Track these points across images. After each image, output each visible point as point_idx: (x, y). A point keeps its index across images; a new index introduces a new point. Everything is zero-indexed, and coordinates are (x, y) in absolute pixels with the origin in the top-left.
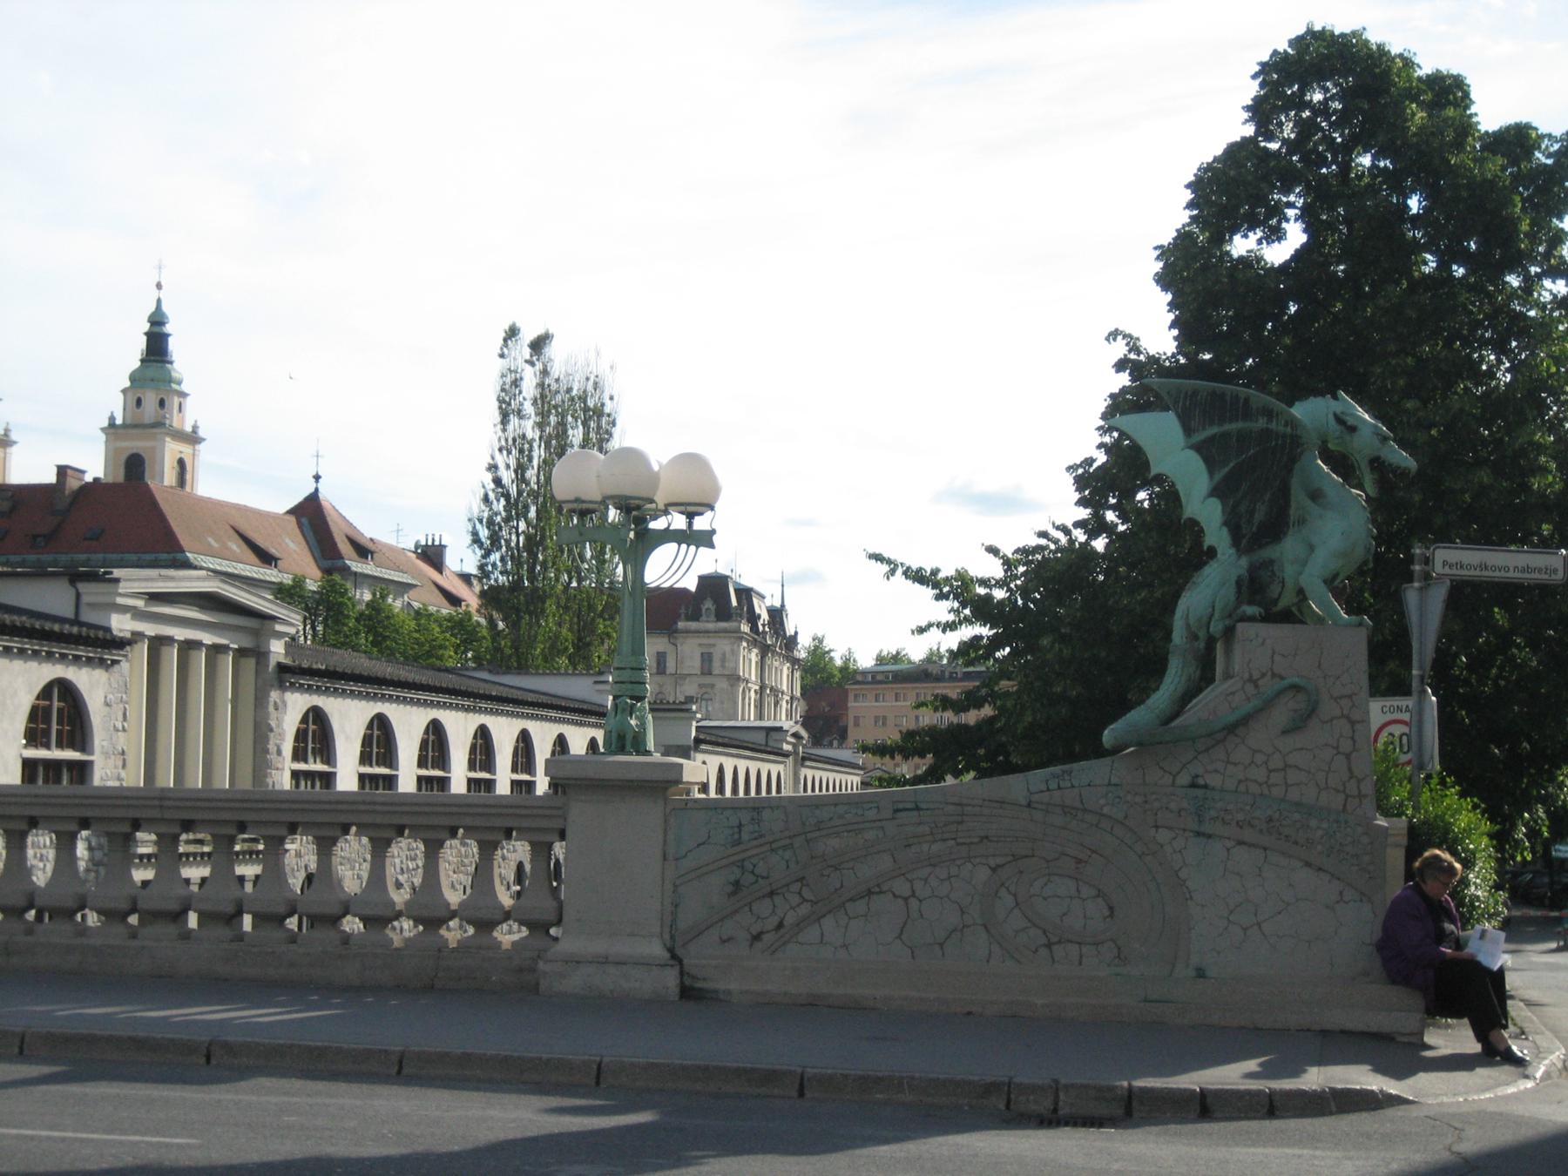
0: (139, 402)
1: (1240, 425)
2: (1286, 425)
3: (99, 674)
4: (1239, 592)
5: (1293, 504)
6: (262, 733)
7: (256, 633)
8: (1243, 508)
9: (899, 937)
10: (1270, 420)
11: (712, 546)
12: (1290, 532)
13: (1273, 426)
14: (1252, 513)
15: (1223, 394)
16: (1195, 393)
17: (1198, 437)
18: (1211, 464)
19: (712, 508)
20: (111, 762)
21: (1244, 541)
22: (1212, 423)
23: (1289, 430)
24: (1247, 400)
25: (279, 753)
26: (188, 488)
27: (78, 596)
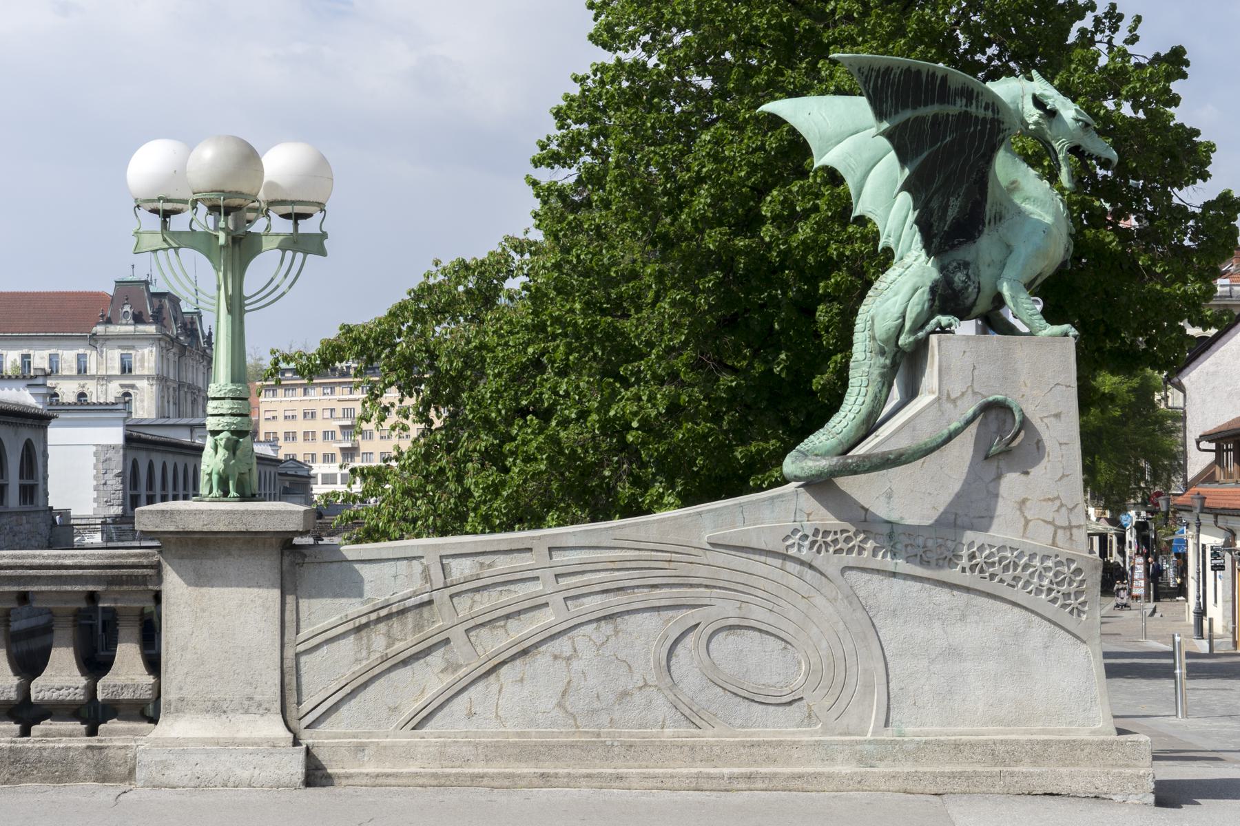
4: (932, 300)
5: (989, 201)
8: (935, 204)
9: (559, 705)
11: (322, 252)
12: (986, 230)
13: (972, 109)
14: (945, 209)
15: (919, 72)
16: (888, 70)
19: (321, 206)
21: (936, 241)
22: (905, 107)
23: (990, 114)
24: (944, 79)
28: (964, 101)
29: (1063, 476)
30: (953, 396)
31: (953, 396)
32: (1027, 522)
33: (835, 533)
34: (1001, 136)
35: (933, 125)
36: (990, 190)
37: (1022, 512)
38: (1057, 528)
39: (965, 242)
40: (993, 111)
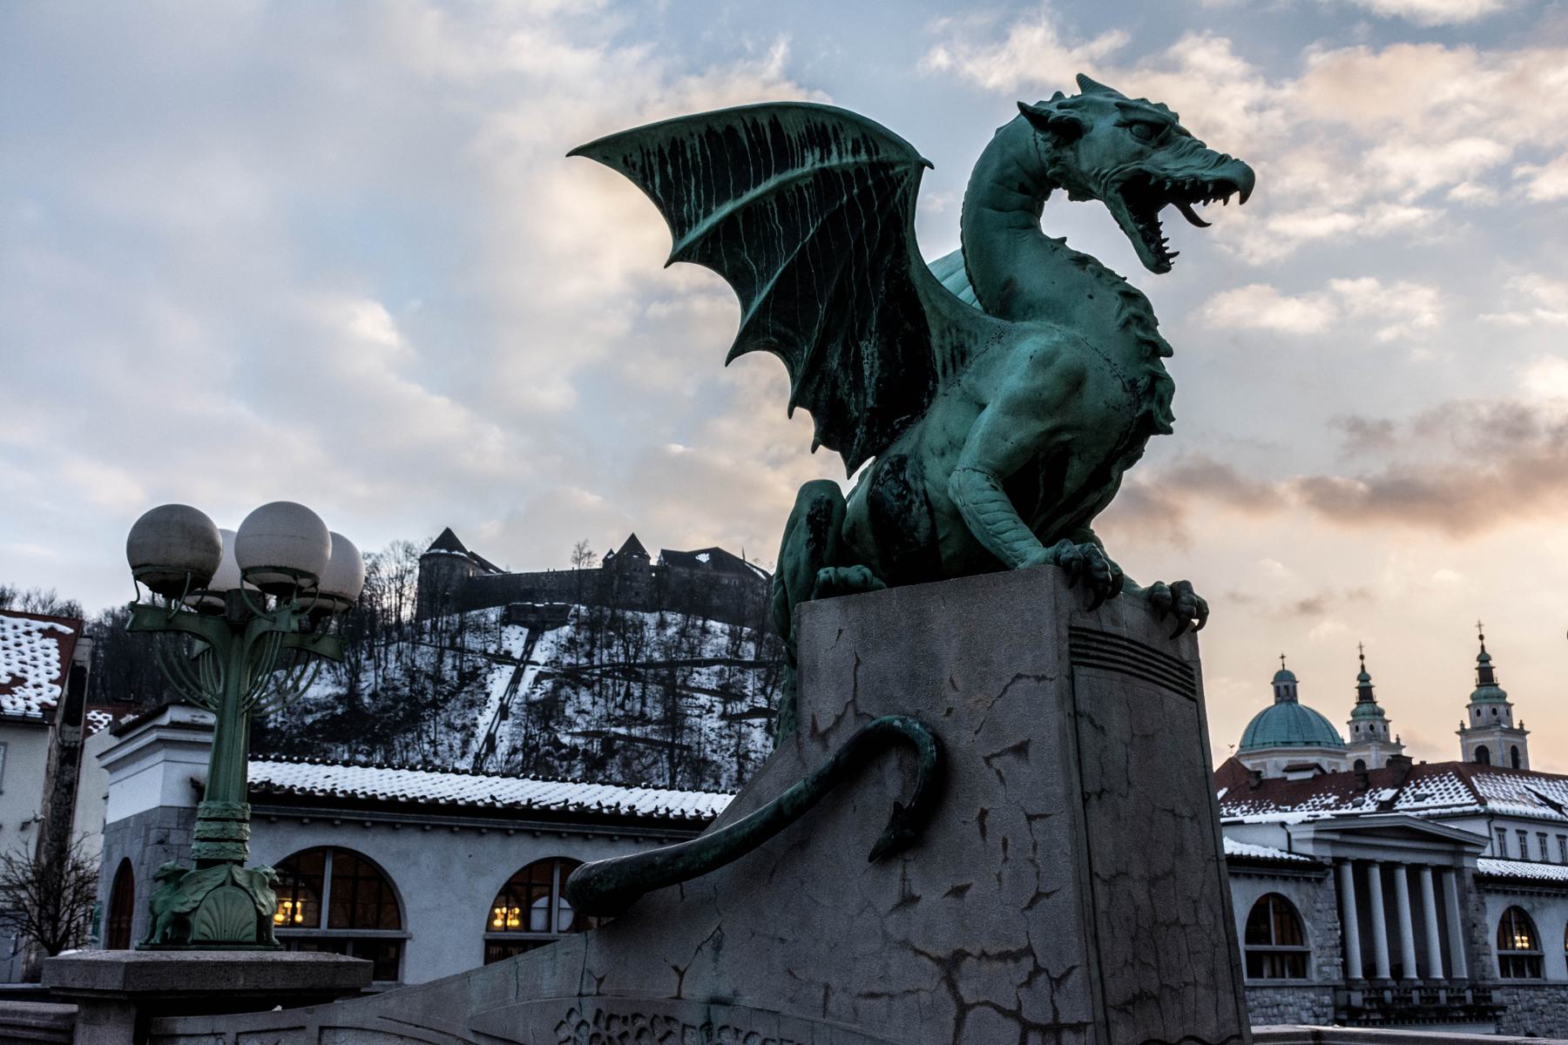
0: (1479, 713)
1: (773, 182)
2: (856, 151)
3: (1307, 889)
5: (934, 332)
6: (1470, 927)
7: (1452, 854)
10: (825, 153)
12: (941, 389)
14: (853, 364)
17: (692, 235)
18: (742, 283)
20: (1327, 952)
25: (1486, 944)
26: (1522, 767)
27: (1289, 835)
28: (817, 152)
29: (1039, 896)
30: (822, 727)
31: (822, 727)
32: (963, 1009)
33: (625, 1019)
34: (899, 191)
35: (783, 220)
36: (926, 307)
37: (953, 987)
38: (1027, 1027)
39: (910, 422)
40: (869, 152)
